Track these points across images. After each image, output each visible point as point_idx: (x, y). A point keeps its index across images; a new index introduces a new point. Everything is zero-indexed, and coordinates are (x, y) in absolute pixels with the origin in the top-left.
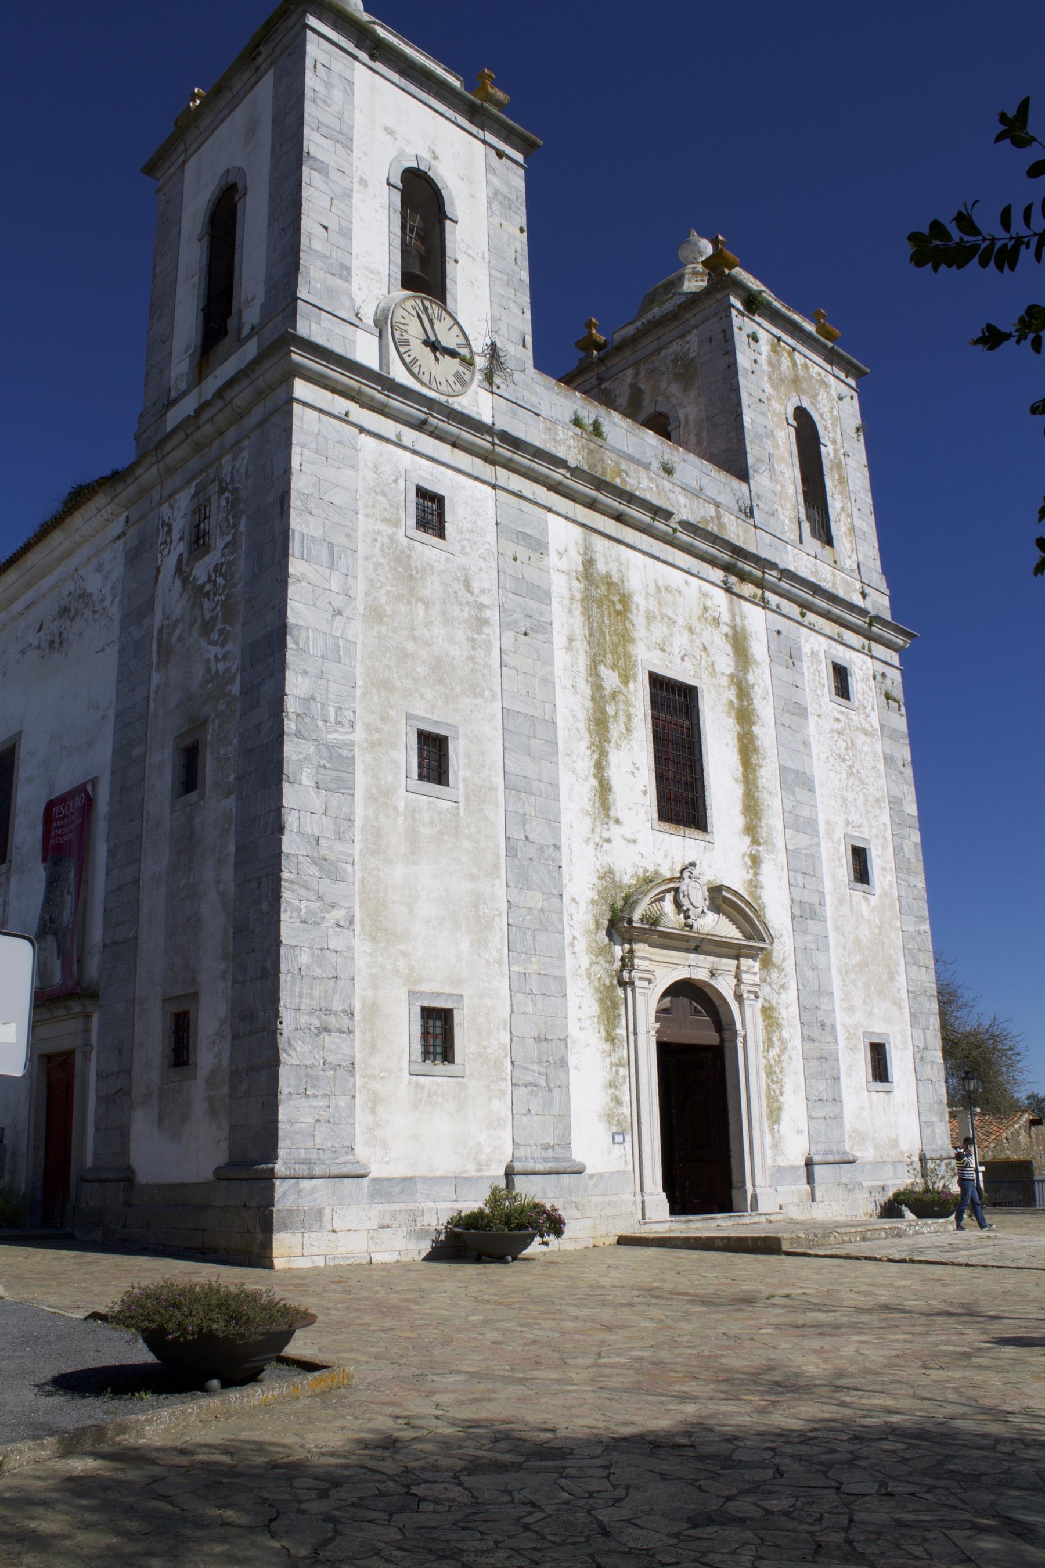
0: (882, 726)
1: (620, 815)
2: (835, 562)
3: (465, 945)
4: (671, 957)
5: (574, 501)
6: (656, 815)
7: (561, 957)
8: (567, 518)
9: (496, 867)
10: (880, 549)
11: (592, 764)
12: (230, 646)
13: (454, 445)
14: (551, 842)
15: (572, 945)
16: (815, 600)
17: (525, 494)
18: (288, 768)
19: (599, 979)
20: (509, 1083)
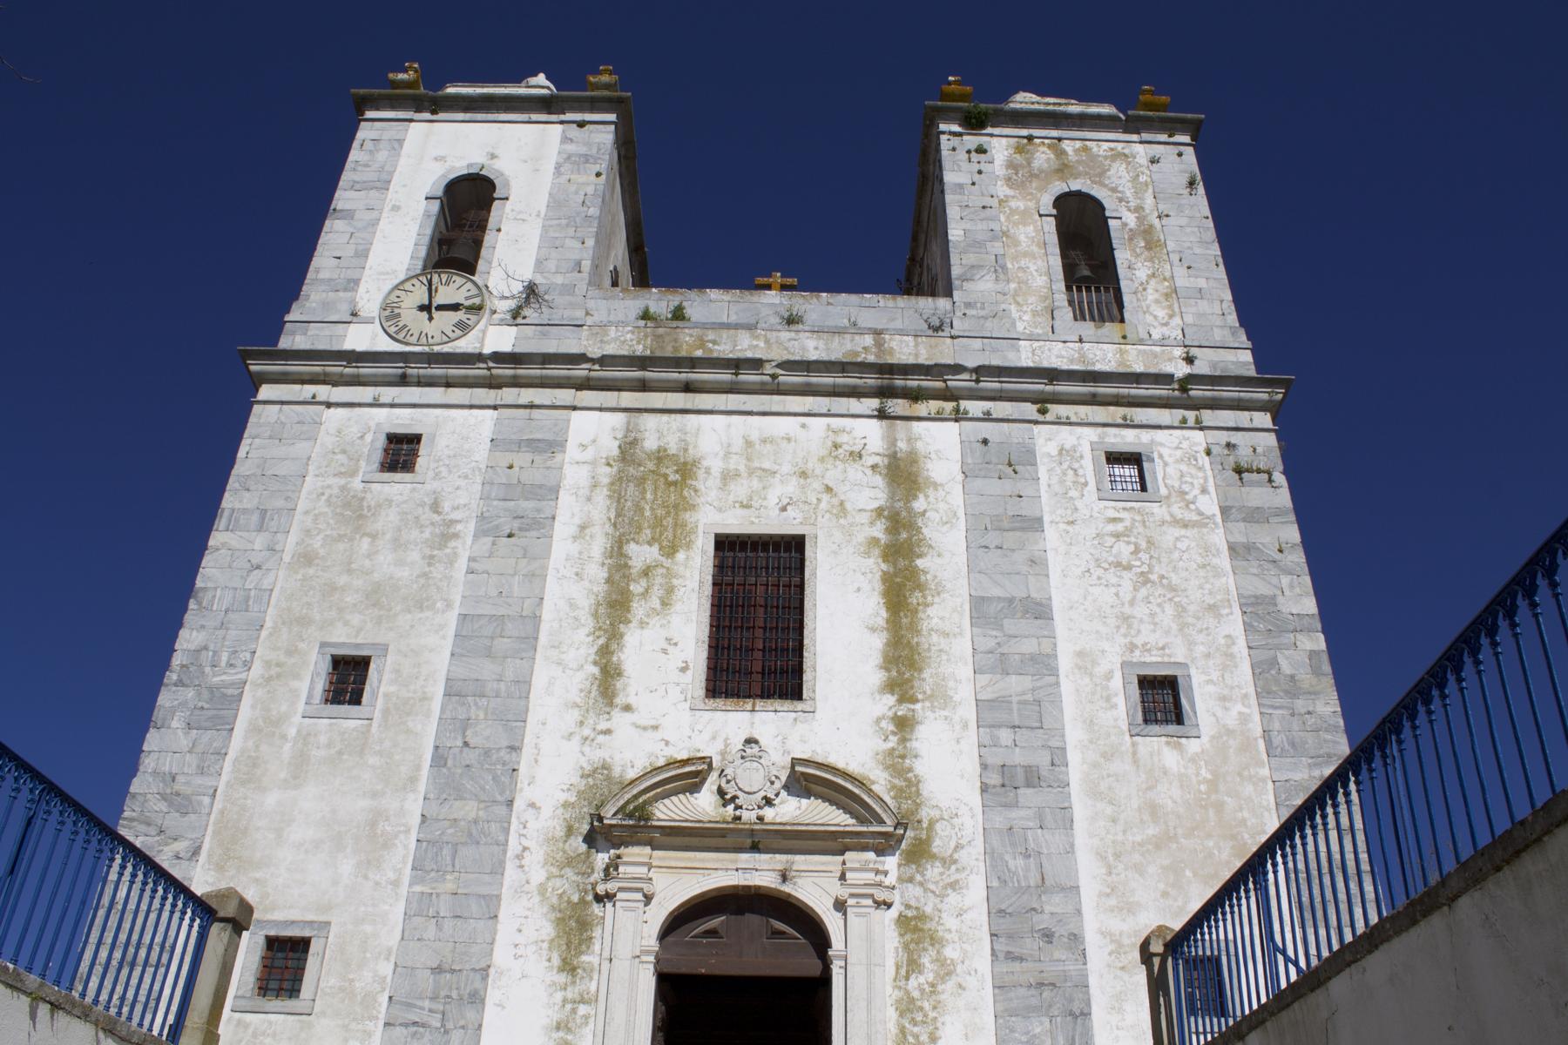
0: (1225, 511)
1: (632, 700)
2: (1124, 337)
3: (347, 867)
4: (702, 860)
5: (620, 390)
6: (702, 692)
7: (498, 870)
8: (601, 409)
9: (413, 780)
10: (1236, 300)
11: (595, 648)
13: (448, 385)
14: (505, 743)
15: (519, 857)
17: (537, 402)
18: (158, 715)
19: (560, 896)
20: (381, 1023)
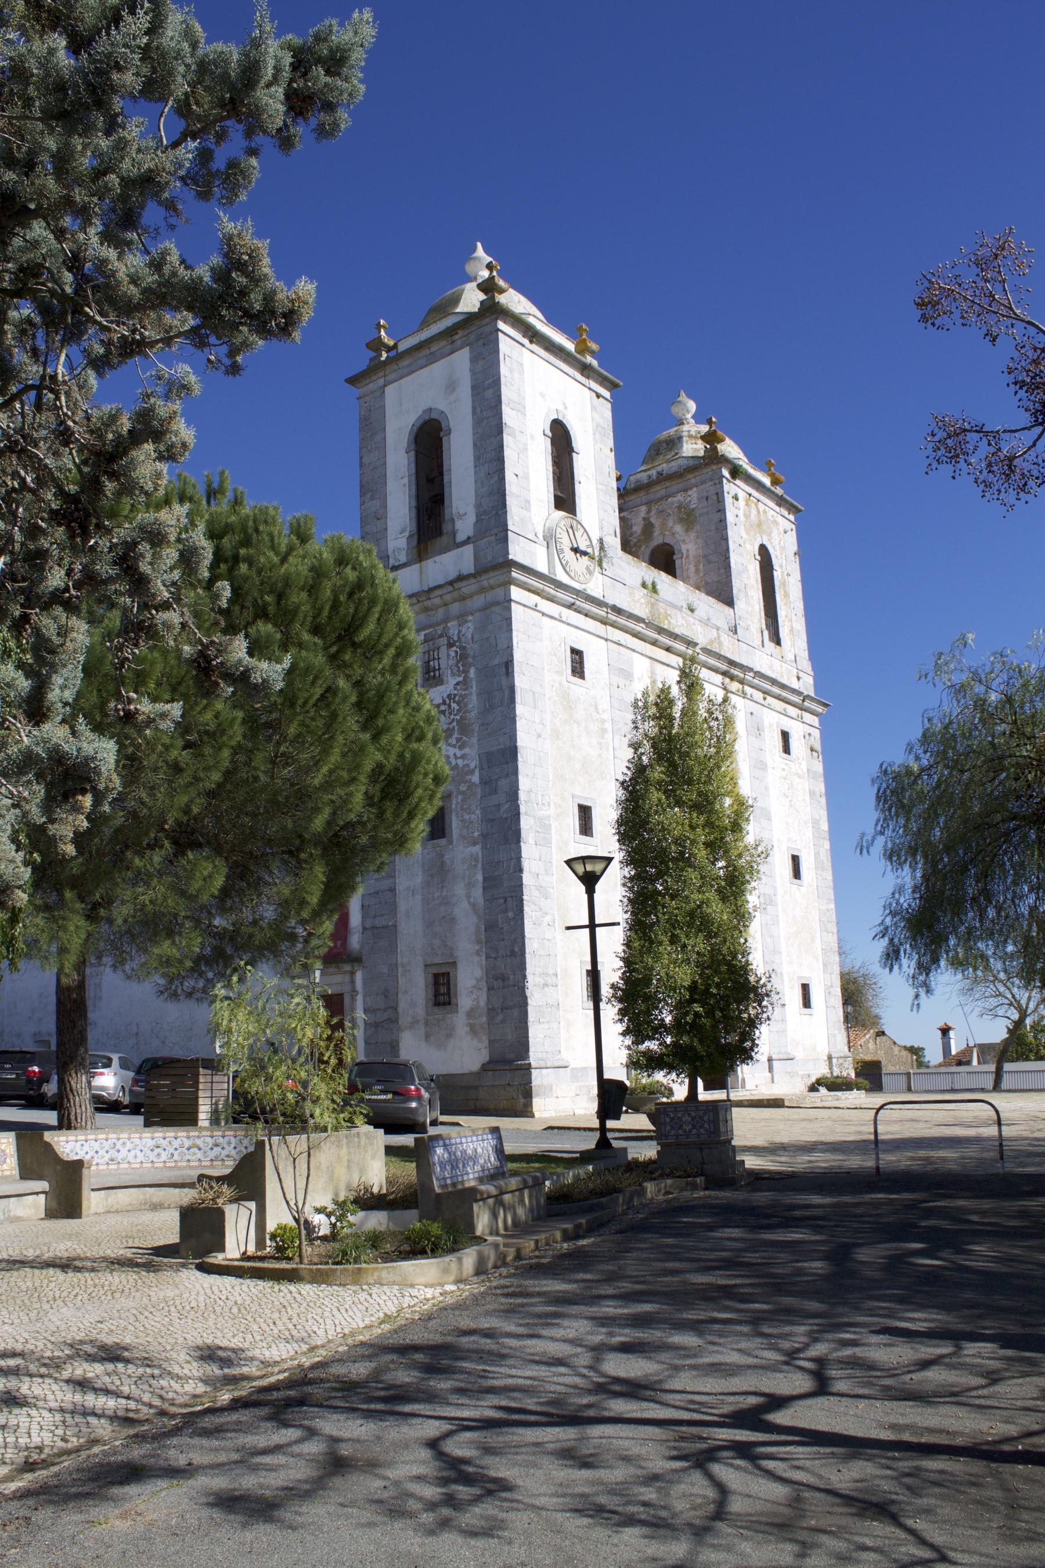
12: (467, 750)
16: (774, 688)
